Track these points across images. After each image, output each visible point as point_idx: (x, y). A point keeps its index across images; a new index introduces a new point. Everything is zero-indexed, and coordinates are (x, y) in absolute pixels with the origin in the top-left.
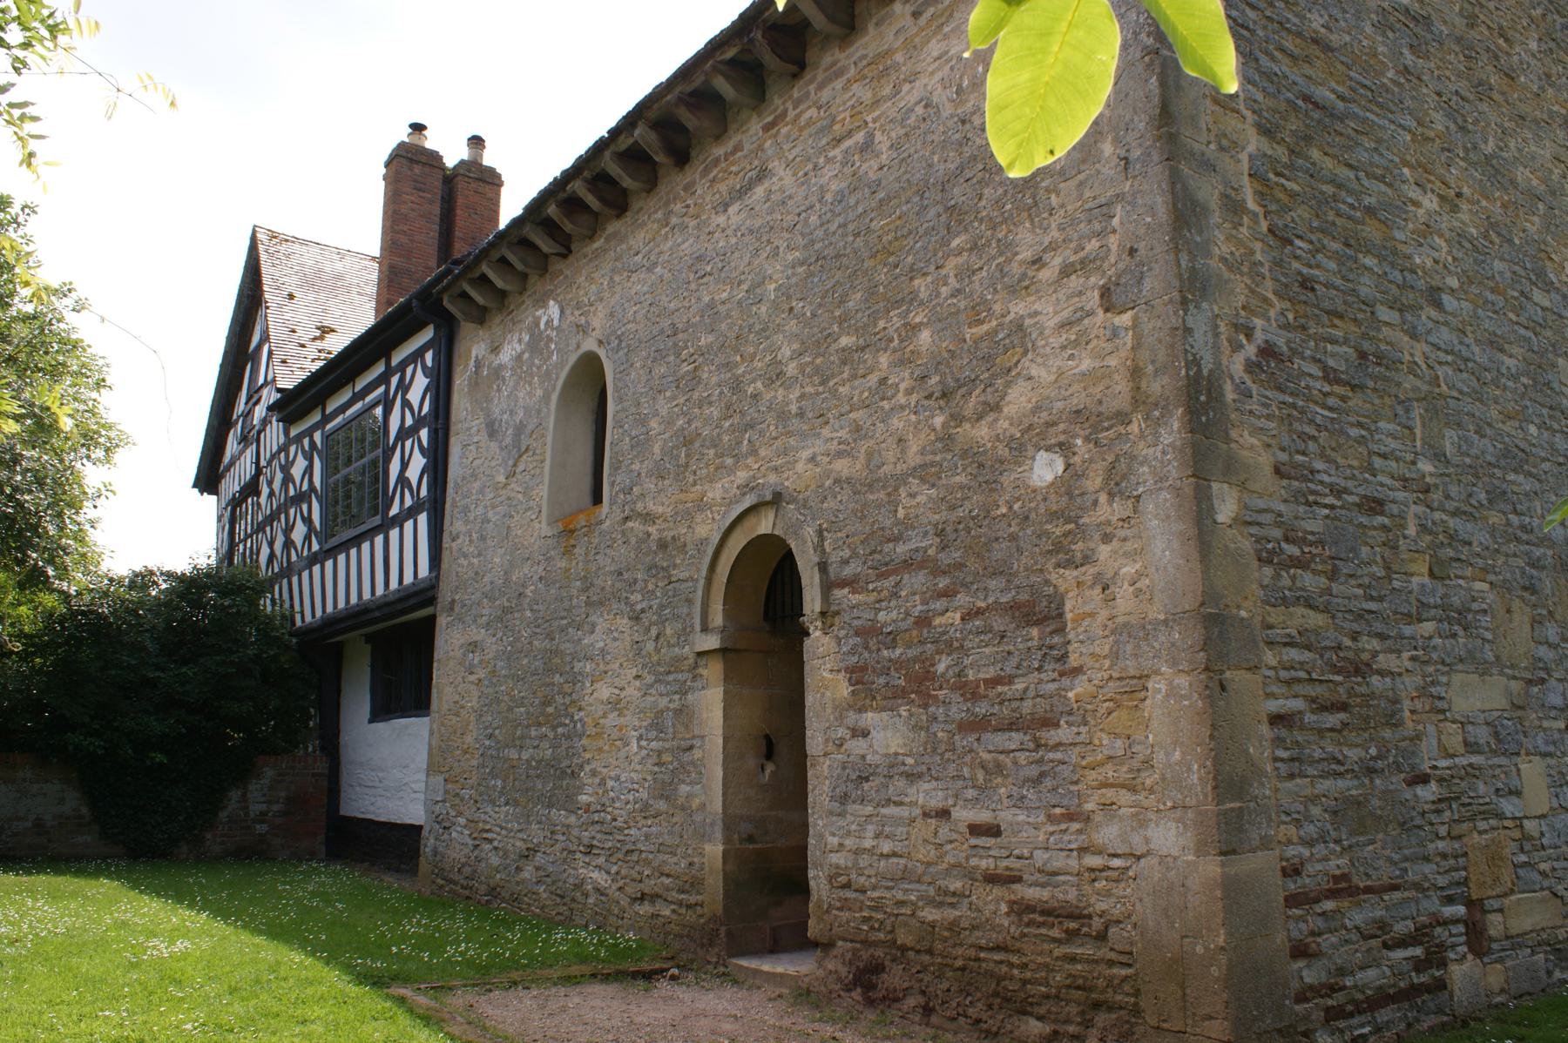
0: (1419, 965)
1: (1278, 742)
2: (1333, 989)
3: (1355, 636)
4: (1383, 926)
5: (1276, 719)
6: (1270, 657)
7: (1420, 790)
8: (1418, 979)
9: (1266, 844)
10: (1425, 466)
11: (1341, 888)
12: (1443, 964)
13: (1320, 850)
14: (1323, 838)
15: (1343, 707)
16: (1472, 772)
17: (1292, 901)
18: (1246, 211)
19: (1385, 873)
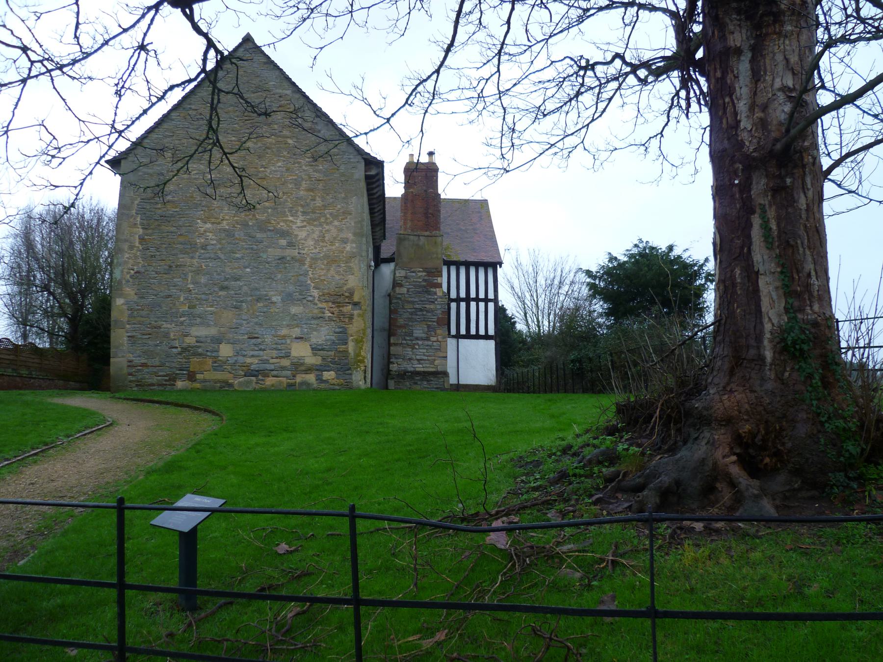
0: (166, 380)
1: (129, 340)
2: (138, 382)
3: (156, 322)
4: (156, 373)
5: (129, 337)
6: (128, 326)
7: (174, 350)
8: (164, 383)
9: (123, 357)
10: (191, 286)
11: (144, 365)
12: (175, 381)
13: (138, 358)
14: (139, 356)
15: (150, 334)
16: (199, 347)
17: (129, 366)
18: (135, 246)
19: (158, 363)
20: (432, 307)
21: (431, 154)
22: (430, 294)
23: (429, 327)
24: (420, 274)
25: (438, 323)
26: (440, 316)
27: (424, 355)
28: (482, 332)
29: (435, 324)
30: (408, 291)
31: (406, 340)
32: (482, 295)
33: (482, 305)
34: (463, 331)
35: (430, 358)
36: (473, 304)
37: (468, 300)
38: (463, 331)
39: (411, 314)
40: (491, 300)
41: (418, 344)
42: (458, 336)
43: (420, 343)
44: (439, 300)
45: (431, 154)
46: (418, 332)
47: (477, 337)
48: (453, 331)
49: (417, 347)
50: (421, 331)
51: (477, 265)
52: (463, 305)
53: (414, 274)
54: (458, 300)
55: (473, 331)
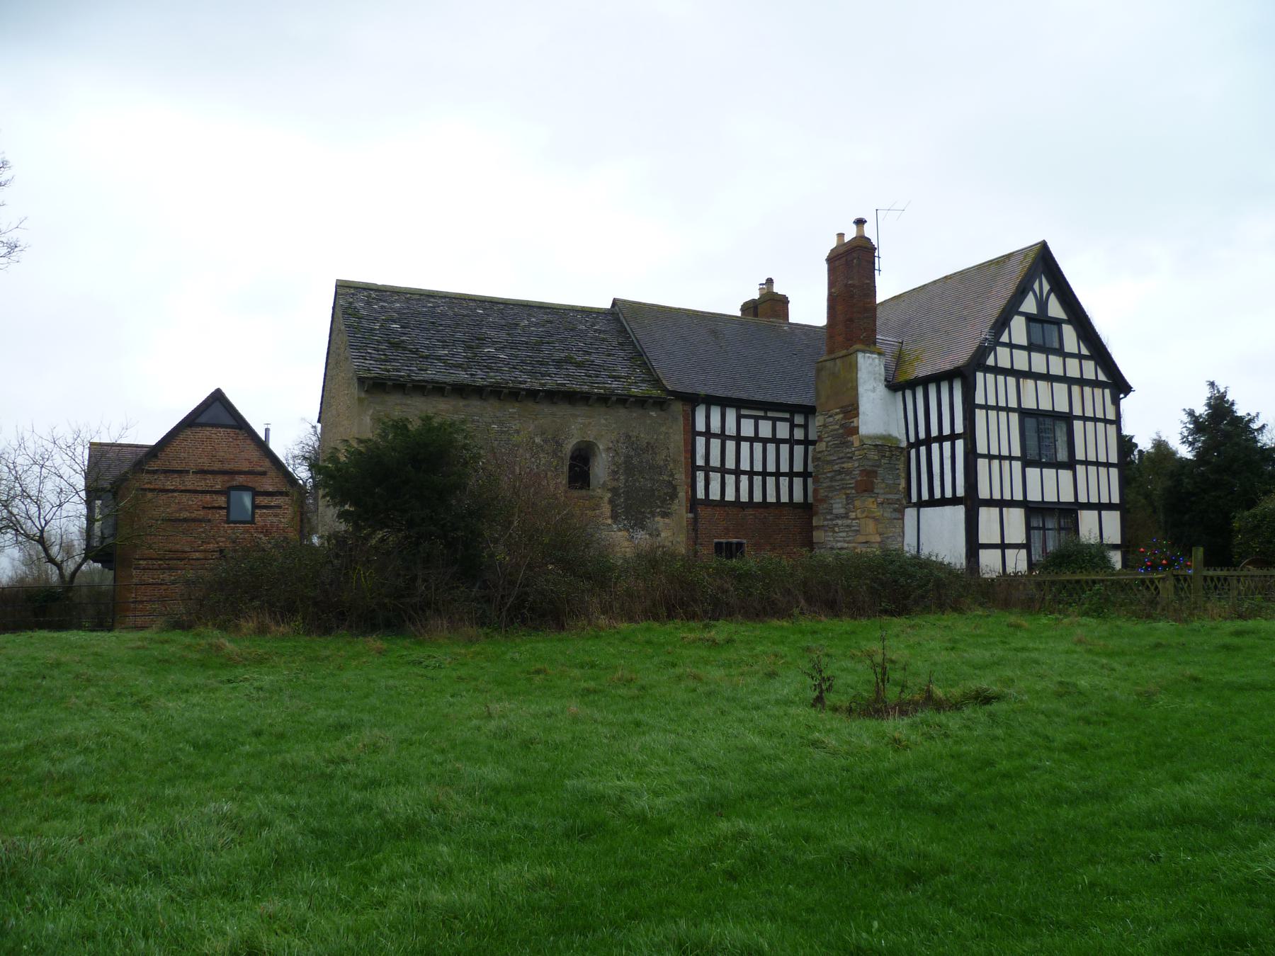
20: (850, 465)
21: (860, 222)
22: (847, 447)
23: (848, 496)
24: (837, 417)
25: (856, 490)
26: (859, 479)
27: (845, 541)
28: (948, 494)
29: (853, 491)
30: (827, 447)
31: (827, 520)
32: (946, 431)
33: (947, 445)
34: (925, 496)
35: (850, 545)
36: (935, 447)
37: (928, 441)
38: (925, 496)
39: (832, 479)
40: (959, 436)
41: (836, 525)
42: (921, 504)
43: (840, 522)
44: (856, 453)
45: (860, 222)
46: (838, 508)
47: (943, 502)
48: (914, 499)
49: (837, 529)
50: (840, 505)
51: (937, 378)
52: (923, 449)
53: (831, 419)
54: (918, 443)
55: (938, 495)
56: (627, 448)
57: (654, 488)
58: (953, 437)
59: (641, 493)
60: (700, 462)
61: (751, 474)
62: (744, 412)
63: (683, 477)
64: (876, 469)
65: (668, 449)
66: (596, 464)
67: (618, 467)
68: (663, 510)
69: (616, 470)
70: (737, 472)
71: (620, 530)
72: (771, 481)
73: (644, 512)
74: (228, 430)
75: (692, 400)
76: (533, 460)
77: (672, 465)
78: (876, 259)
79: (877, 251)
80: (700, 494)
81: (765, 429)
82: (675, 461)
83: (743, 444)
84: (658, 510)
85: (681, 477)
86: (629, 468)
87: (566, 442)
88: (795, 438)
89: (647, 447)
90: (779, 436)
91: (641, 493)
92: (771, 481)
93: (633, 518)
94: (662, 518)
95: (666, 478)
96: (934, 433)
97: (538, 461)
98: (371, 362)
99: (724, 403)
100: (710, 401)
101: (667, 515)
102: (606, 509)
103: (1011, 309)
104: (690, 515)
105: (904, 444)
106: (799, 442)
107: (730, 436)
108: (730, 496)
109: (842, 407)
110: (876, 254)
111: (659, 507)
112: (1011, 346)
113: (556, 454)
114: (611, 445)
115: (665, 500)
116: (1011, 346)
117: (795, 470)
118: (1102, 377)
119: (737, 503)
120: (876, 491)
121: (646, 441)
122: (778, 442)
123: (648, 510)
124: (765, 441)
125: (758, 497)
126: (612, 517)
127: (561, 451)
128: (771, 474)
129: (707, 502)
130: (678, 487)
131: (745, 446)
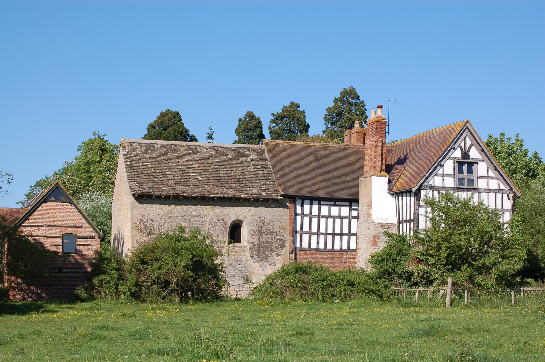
56: (259, 222)
57: (273, 242)
58: (410, 221)
59: (266, 245)
60: (298, 229)
61: (326, 234)
62: (322, 203)
63: (288, 236)
64: (379, 234)
65: (281, 223)
66: (244, 230)
67: (255, 232)
68: (277, 253)
69: (253, 233)
70: (318, 234)
71: (255, 263)
72: (337, 238)
73: (267, 254)
74: (63, 203)
75: (293, 199)
76: (212, 229)
77: (282, 231)
78: (387, 127)
79: (387, 123)
80: (298, 245)
81: (335, 211)
82: (284, 228)
83: (322, 219)
84: (275, 253)
85: (288, 237)
86: (260, 233)
87: (228, 220)
88: (352, 215)
89: (270, 222)
90: (343, 214)
91: (266, 245)
92: (337, 238)
93: (262, 257)
94: (277, 256)
95: (279, 237)
96: (405, 219)
97: (215, 230)
98: (137, 184)
99: (312, 200)
100: (303, 199)
101: (280, 256)
102: (248, 253)
103: (445, 156)
104: (293, 255)
105: (395, 221)
106: (354, 218)
107: (315, 216)
108: (314, 246)
109: (367, 203)
110: (387, 124)
111: (275, 251)
112: (443, 175)
113: (223, 226)
114: (251, 221)
115: (279, 248)
116: (443, 175)
117: (352, 232)
118: (502, 187)
119: (318, 250)
120: (378, 245)
121: (269, 219)
122: (342, 218)
123: (270, 253)
124: (334, 218)
125: (329, 246)
126: (251, 256)
127: (226, 225)
128: (338, 234)
129: (301, 249)
130: (285, 241)
131: (323, 221)
